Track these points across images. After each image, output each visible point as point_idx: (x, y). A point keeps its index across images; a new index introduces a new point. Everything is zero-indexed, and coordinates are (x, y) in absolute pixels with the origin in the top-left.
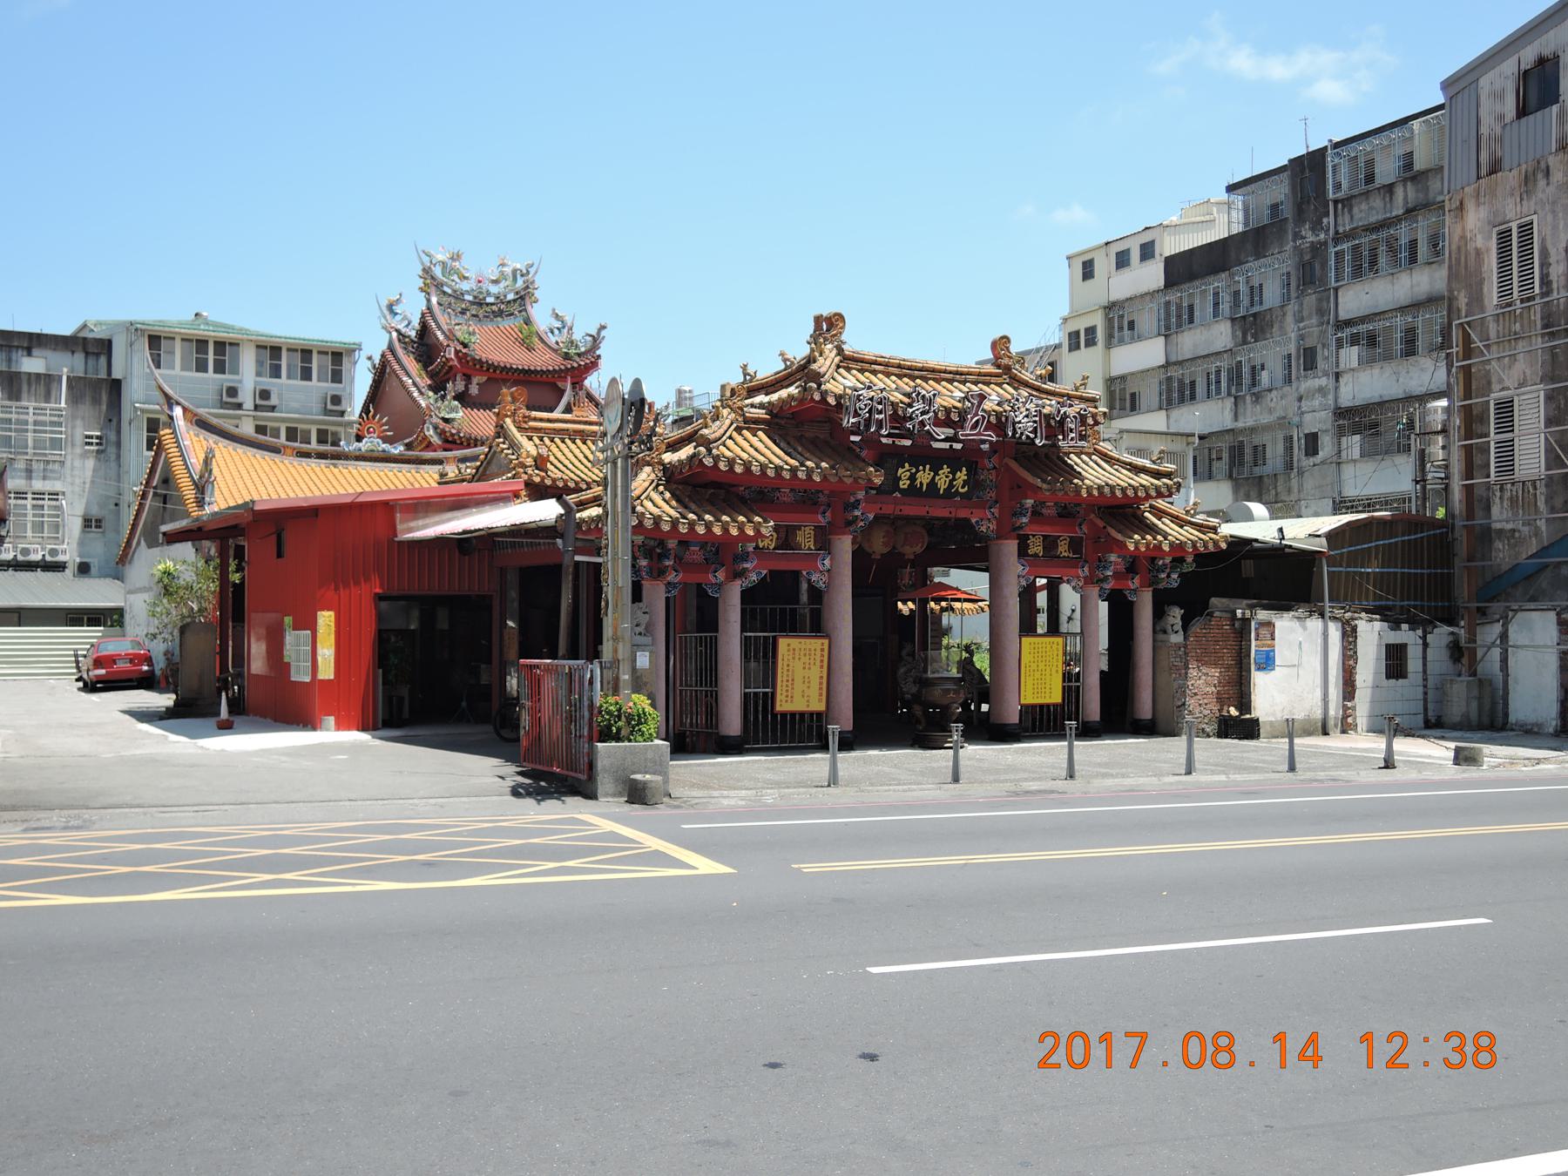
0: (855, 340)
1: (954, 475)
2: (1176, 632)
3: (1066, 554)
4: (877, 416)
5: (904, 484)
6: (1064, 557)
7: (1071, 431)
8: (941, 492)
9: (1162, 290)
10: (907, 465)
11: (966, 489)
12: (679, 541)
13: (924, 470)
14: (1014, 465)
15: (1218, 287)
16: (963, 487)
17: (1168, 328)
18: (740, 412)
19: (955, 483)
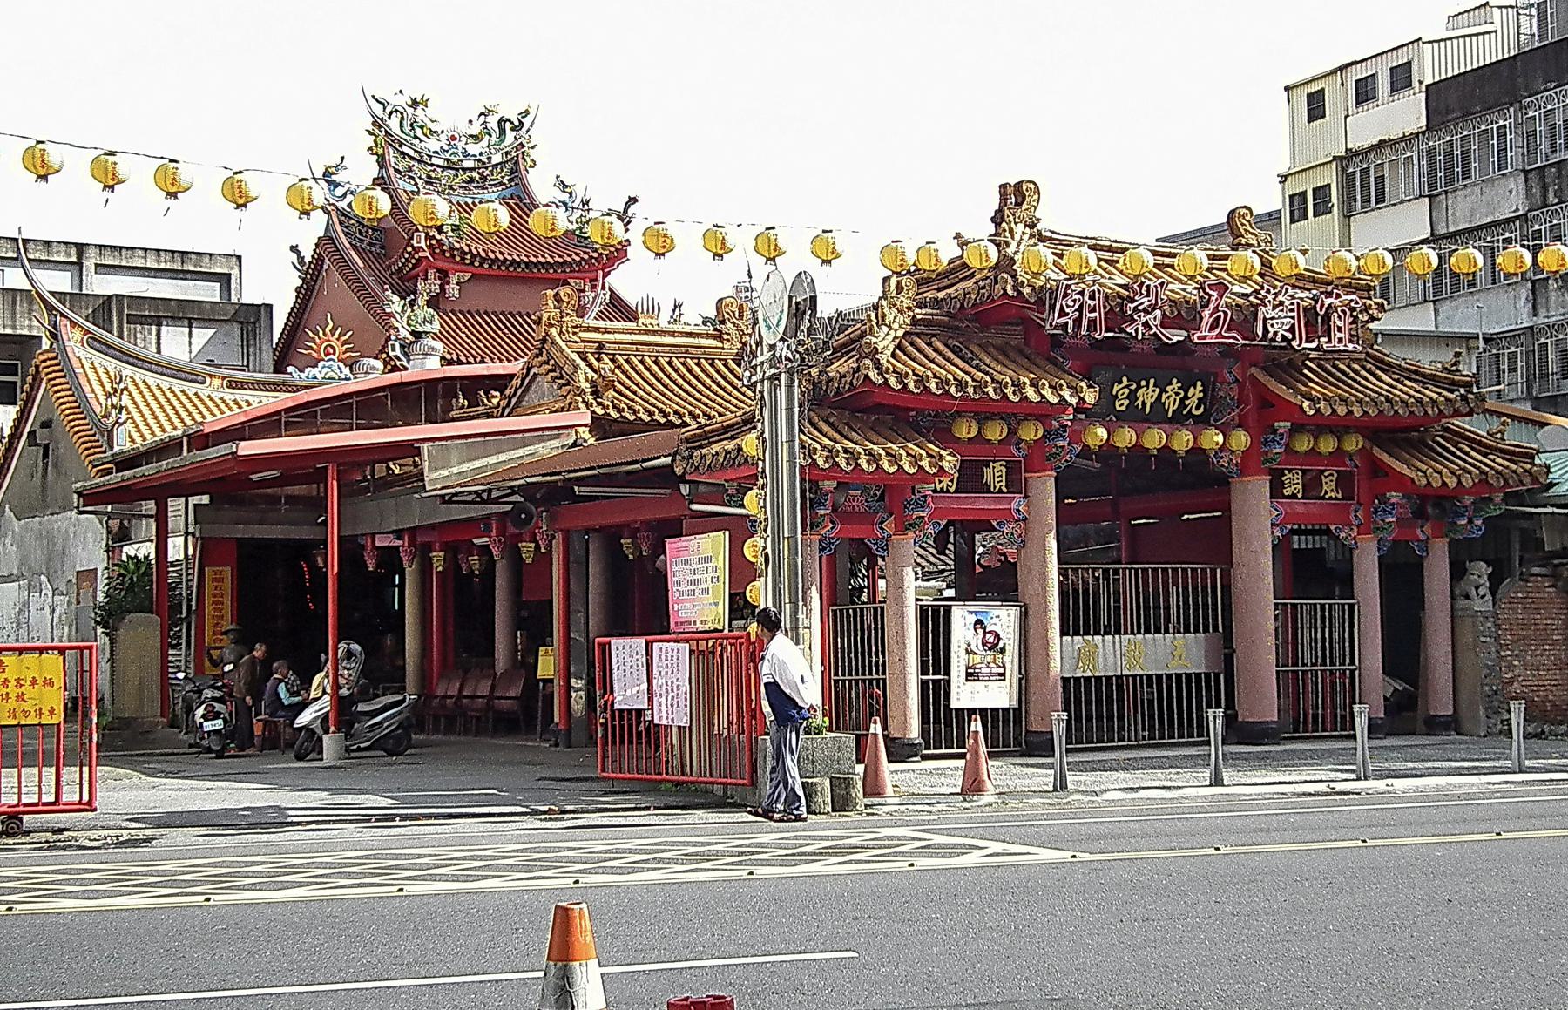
0: (1050, 217)
1: (1186, 392)
2: (1483, 597)
3: (1333, 495)
4: (1089, 315)
5: (1121, 405)
6: (1331, 498)
7: (1340, 329)
8: (1170, 414)
9: (1423, 133)
10: (1125, 379)
11: (1202, 410)
12: (839, 483)
13: (1147, 386)
14: (1263, 378)
15: (1505, 126)
16: (1198, 408)
17: (1433, 186)
18: (1514, 280)
19: (1187, 402)
